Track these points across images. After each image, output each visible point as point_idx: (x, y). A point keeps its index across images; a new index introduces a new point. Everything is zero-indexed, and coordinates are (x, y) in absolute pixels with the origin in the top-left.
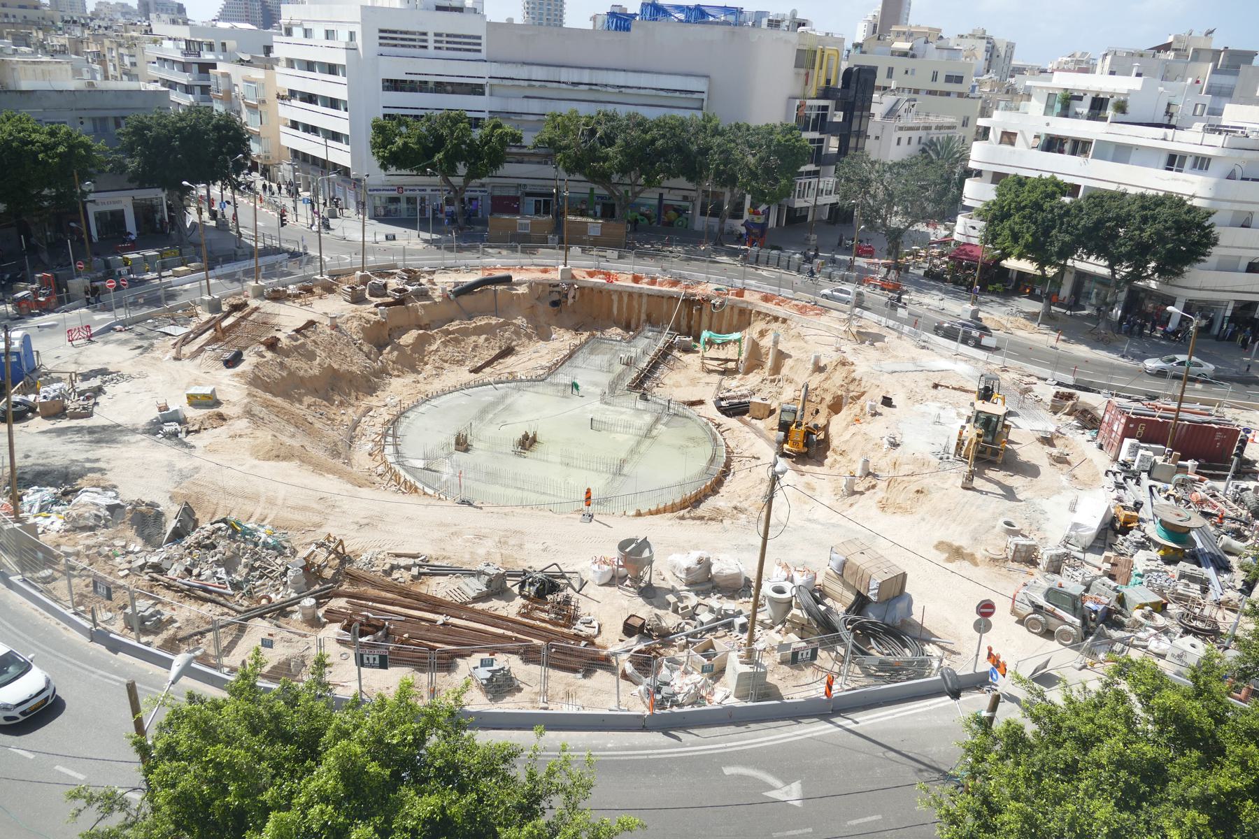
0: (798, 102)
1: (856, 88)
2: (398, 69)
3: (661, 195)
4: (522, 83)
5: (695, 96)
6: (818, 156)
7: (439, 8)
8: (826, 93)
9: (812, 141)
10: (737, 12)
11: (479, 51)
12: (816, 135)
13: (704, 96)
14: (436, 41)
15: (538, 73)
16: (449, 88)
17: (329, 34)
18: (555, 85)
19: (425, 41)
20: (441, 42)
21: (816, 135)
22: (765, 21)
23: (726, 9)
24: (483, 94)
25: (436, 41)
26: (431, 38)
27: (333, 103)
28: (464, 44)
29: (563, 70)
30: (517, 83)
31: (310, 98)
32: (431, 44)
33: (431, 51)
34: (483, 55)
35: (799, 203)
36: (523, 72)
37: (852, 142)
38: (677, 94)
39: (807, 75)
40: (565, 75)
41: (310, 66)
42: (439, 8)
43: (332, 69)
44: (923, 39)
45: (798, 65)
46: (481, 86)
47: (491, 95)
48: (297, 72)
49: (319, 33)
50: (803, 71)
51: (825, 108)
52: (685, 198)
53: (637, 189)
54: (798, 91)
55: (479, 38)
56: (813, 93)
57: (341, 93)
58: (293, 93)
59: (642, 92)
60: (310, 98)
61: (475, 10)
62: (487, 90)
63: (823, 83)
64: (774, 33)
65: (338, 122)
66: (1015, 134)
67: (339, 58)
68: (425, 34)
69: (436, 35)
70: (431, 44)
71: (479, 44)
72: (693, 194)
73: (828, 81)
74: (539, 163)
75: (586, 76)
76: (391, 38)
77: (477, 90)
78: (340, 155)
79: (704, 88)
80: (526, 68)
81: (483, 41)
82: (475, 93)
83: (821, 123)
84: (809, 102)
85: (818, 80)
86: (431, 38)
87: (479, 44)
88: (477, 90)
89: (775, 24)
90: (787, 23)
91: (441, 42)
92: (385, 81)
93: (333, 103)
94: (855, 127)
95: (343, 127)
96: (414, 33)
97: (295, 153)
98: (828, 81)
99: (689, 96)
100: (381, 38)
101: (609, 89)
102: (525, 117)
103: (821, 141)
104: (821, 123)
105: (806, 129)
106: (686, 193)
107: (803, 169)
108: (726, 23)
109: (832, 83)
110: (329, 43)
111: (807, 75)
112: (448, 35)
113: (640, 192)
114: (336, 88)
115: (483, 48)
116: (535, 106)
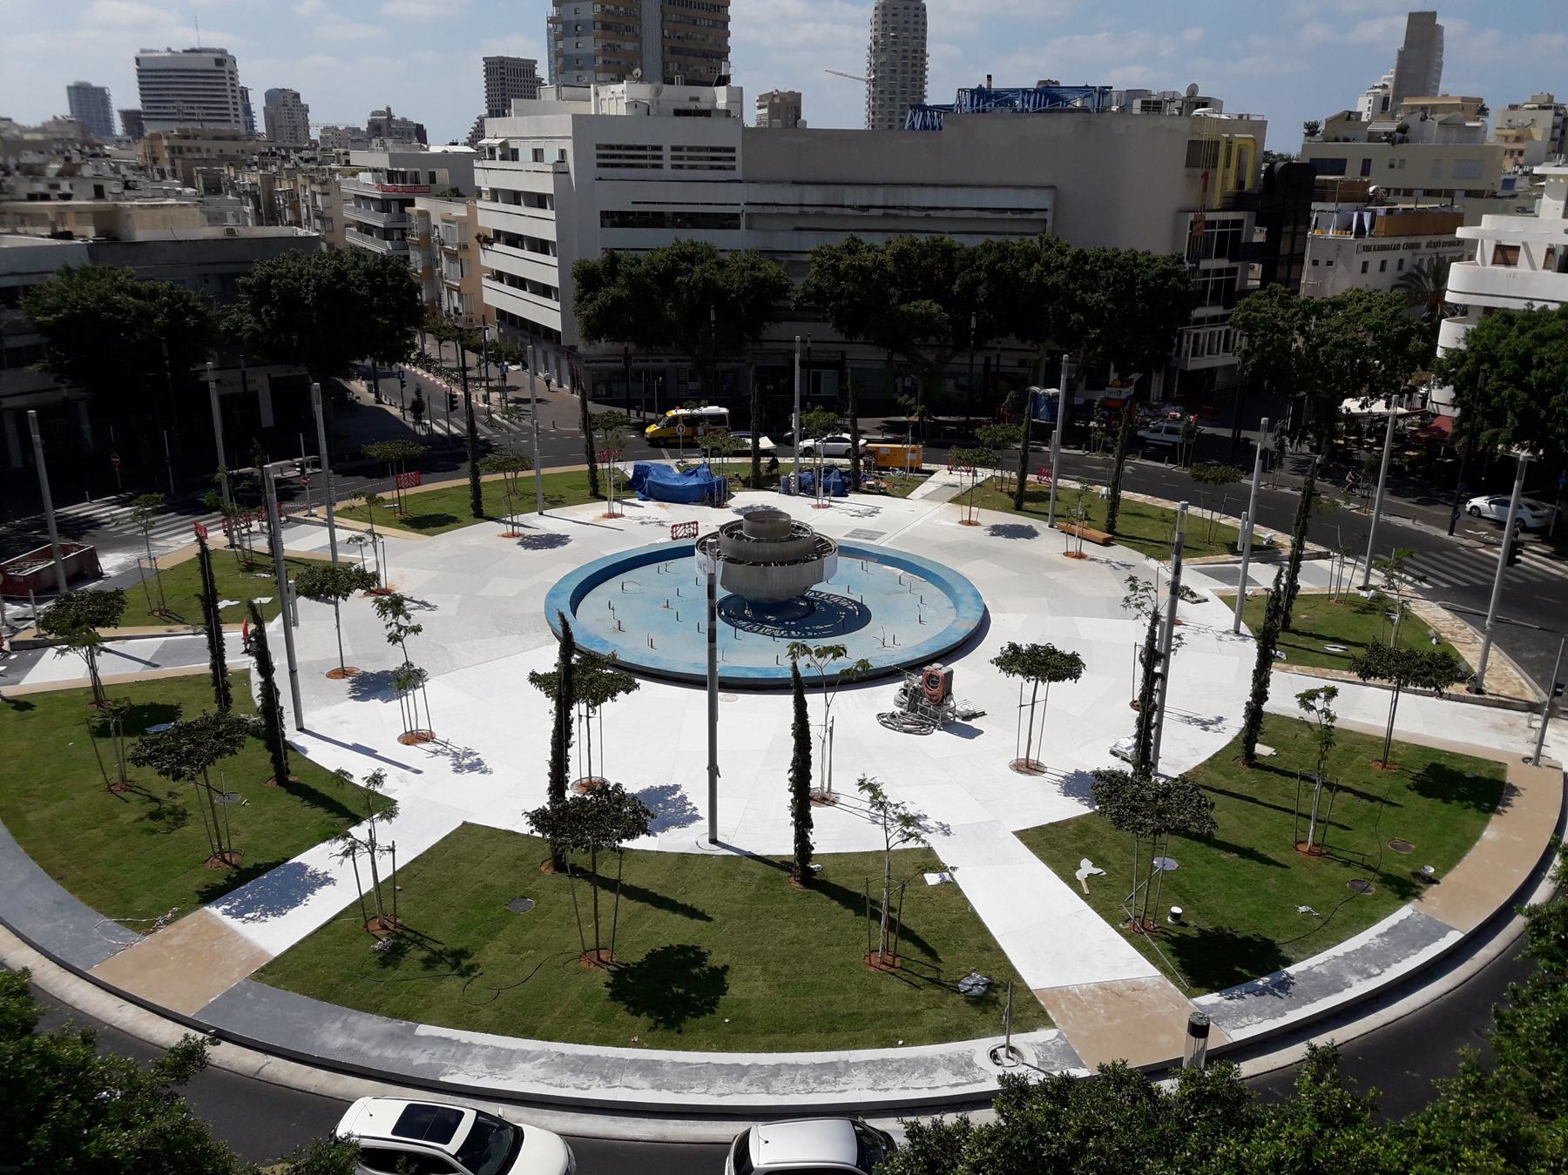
0: (1191, 217)
1: (1286, 194)
2: (622, 198)
3: (988, 360)
4: (791, 210)
5: (1033, 216)
6: (1227, 292)
7: (678, 113)
8: (1238, 201)
9: (1219, 272)
10: (1104, 92)
11: (733, 168)
12: (1224, 263)
13: (1048, 216)
15: (813, 195)
17: (538, 155)
18: (836, 211)
19: (660, 158)
20: (681, 158)
21: (1224, 263)
22: (1137, 103)
23: (1086, 91)
24: (738, 227)
25: (673, 158)
27: (541, 246)
28: (719, 157)
29: (848, 189)
30: (783, 210)
31: (514, 240)
32: (667, 162)
33: (667, 171)
34: (738, 174)
35: (1194, 364)
36: (789, 195)
37: (1281, 271)
38: (1009, 215)
39: (1205, 176)
40: (852, 196)
41: (515, 197)
42: (678, 113)
43: (540, 201)
44: (1420, 114)
45: (1191, 163)
46: (736, 216)
47: (749, 228)
48: (500, 206)
49: (526, 153)
50: (1199, 172)
51: (1239, 223)
52: (1022, 363)
53: (948, 352)
54: (1192, 200)
55: (732, 150)
56: (1216, 202)
57: (548, 232)
58: (498, 233)
59: (958, 214)
60: (514, 240)
61: (727, 113)
62: (743, 221)
63: (1231, 186)
64: (1154, 120)
65: (546, 270)
66: (1517, 248)
67: (545, 185)
68: (659, 148)
69: (674, 149)
70: (667, 162)
71: (733, 159)
72: (1034, 356)
73: (1241, 184)
74: (817, 320)
75: (879, 197)
77: (727, 221)
78: (548, 315)
79: (1047, 204)
80: (796, 188)
81: (738, 154)
82: (729, 227)
83: (1231, 244)
84: (1209, 216)
85: (1224, 181)
86: (667, 153)
87: (733, 159)
88: (727, 221)
89: (1153, 106)
90: (1178, 103)
91: (681, 158)
92: (606, 215)
93: (541, 246)
94: (1285, 249)
95: (551, 278)
96: (644, 148)
98: (1241, 184)
99: (1025, 216)
100: (599, 156)
101: (913, 213)
102: (796, 257)
103: (1233, 271)
104: (1231, 244)
105: (1207, 256)
106: (1023, 355)
107: (1198, 313)
108: (1084, 110)
109: (1248, 186)
110: (538, 166)
111: (1205, 176)
112: (690, 149)
113: (951, 357)
114: (543, 225)
115: (738, 163)
116: (810, 242)
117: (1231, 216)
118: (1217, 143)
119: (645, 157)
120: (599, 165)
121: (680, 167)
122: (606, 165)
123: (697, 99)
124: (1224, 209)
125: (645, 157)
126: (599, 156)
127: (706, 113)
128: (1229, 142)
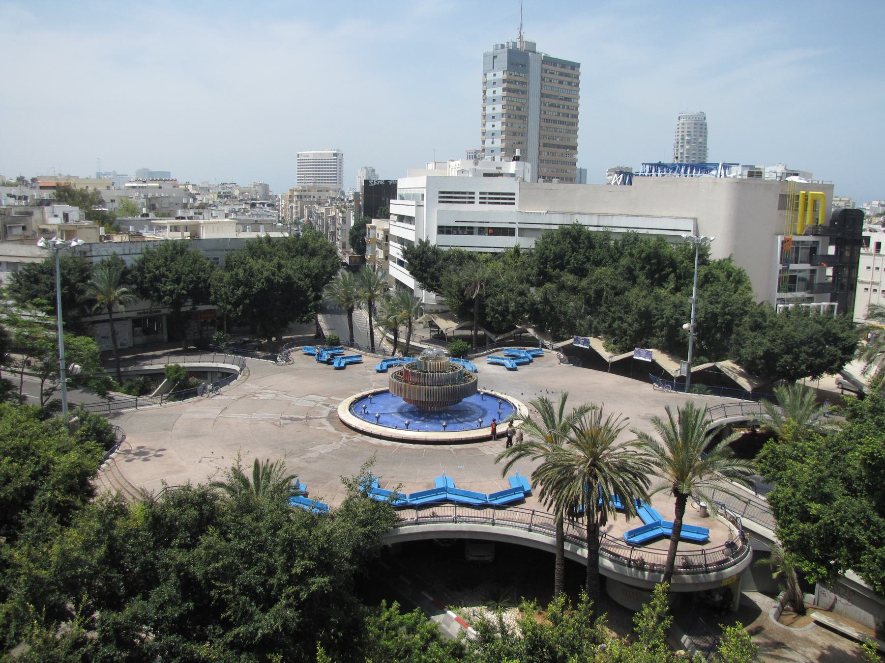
7: (485, 175)
8: (815, 230)
11: (514, 204)
14: (481, 198)
16: (491, 231)
20: (485, 198)
26: (477, 196)
42: (485, 175)
45: (782, 206)
55: (514, 194)
63: (809, 221)
68: (473, 193)
69: (481, 193)
76: (448, 197)
79: (691, 228)
84: (795, 238)
91: (485, 198)
96: (465, 193)
97: (398, 282)
100: (440, 197)
112: (490, 193)
115: (516, 201)
117: (810, 238)
118: (798, 196)
119: (465, 198)
120: (440, 202)
121: (484, 203)
122: (443, 202)
123: (500, 168)
124: (805, 234)
125: (465, 198)
126: (440, 197)
127: (501, 175)
128: (806, 196)
